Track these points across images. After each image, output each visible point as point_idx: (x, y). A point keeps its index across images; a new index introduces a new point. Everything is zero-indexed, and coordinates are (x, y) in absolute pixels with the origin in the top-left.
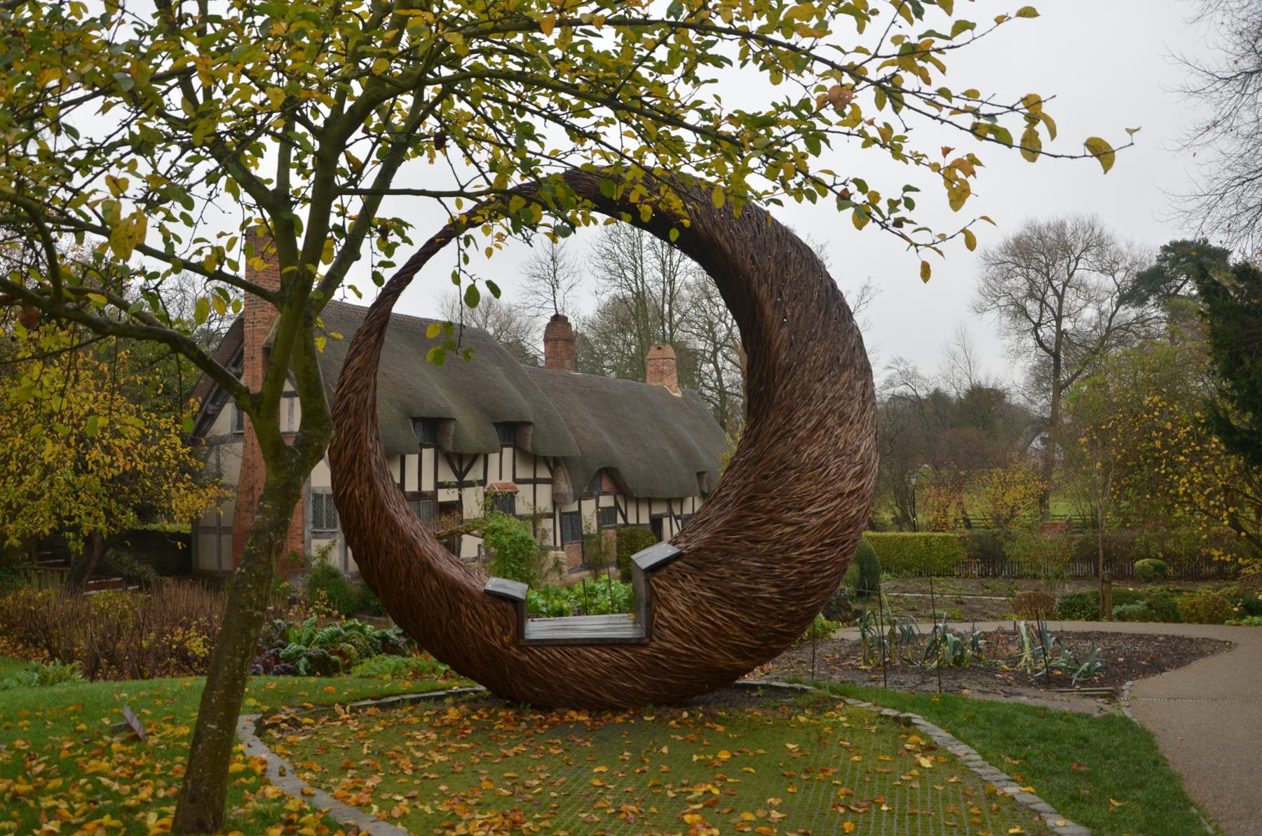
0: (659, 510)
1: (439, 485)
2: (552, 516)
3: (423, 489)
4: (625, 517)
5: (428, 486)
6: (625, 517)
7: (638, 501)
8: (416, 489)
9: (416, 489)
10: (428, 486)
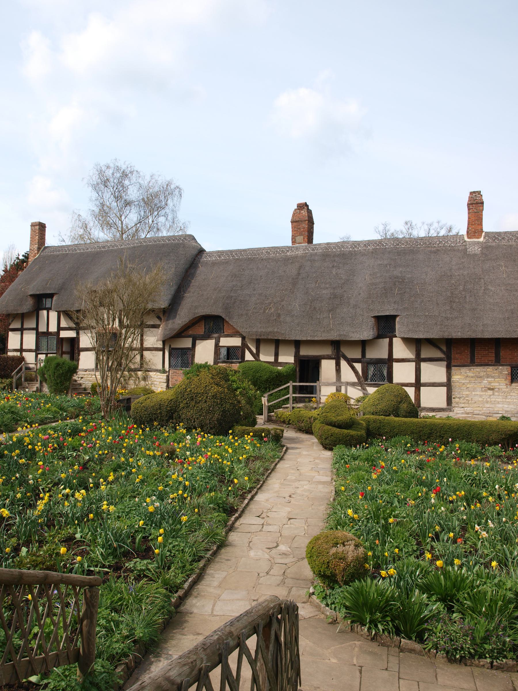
0: (305, 352)
1: (59, 329)
2: (163, 350)
3: (50, 330)
4: (256, 356)
5: (53, 328)
6: (256, 356)
7: (278, 344)
8: (45, 330)
9: (46, 331)
10: (53, 328)
